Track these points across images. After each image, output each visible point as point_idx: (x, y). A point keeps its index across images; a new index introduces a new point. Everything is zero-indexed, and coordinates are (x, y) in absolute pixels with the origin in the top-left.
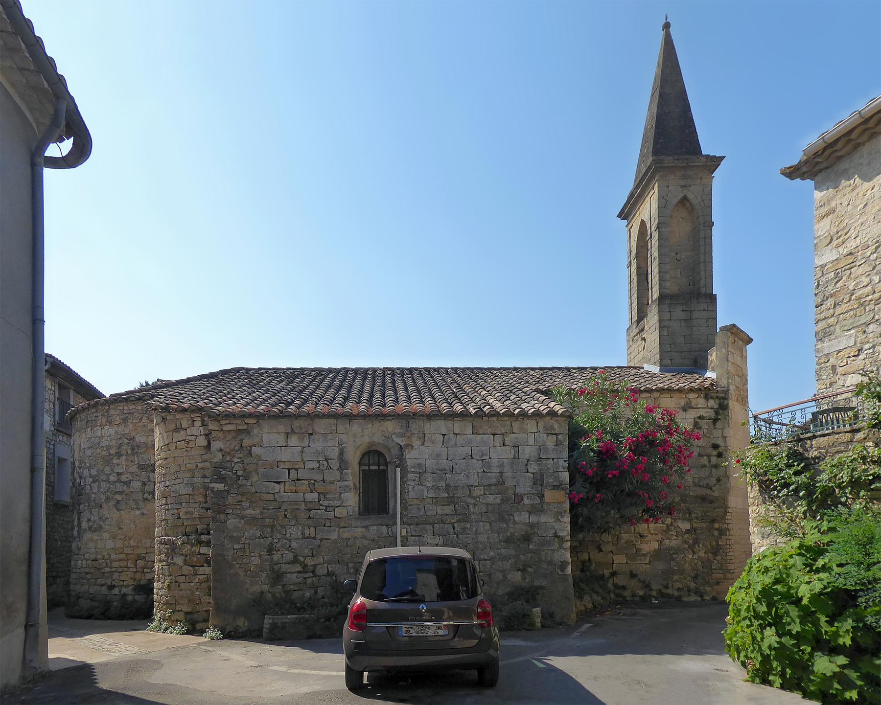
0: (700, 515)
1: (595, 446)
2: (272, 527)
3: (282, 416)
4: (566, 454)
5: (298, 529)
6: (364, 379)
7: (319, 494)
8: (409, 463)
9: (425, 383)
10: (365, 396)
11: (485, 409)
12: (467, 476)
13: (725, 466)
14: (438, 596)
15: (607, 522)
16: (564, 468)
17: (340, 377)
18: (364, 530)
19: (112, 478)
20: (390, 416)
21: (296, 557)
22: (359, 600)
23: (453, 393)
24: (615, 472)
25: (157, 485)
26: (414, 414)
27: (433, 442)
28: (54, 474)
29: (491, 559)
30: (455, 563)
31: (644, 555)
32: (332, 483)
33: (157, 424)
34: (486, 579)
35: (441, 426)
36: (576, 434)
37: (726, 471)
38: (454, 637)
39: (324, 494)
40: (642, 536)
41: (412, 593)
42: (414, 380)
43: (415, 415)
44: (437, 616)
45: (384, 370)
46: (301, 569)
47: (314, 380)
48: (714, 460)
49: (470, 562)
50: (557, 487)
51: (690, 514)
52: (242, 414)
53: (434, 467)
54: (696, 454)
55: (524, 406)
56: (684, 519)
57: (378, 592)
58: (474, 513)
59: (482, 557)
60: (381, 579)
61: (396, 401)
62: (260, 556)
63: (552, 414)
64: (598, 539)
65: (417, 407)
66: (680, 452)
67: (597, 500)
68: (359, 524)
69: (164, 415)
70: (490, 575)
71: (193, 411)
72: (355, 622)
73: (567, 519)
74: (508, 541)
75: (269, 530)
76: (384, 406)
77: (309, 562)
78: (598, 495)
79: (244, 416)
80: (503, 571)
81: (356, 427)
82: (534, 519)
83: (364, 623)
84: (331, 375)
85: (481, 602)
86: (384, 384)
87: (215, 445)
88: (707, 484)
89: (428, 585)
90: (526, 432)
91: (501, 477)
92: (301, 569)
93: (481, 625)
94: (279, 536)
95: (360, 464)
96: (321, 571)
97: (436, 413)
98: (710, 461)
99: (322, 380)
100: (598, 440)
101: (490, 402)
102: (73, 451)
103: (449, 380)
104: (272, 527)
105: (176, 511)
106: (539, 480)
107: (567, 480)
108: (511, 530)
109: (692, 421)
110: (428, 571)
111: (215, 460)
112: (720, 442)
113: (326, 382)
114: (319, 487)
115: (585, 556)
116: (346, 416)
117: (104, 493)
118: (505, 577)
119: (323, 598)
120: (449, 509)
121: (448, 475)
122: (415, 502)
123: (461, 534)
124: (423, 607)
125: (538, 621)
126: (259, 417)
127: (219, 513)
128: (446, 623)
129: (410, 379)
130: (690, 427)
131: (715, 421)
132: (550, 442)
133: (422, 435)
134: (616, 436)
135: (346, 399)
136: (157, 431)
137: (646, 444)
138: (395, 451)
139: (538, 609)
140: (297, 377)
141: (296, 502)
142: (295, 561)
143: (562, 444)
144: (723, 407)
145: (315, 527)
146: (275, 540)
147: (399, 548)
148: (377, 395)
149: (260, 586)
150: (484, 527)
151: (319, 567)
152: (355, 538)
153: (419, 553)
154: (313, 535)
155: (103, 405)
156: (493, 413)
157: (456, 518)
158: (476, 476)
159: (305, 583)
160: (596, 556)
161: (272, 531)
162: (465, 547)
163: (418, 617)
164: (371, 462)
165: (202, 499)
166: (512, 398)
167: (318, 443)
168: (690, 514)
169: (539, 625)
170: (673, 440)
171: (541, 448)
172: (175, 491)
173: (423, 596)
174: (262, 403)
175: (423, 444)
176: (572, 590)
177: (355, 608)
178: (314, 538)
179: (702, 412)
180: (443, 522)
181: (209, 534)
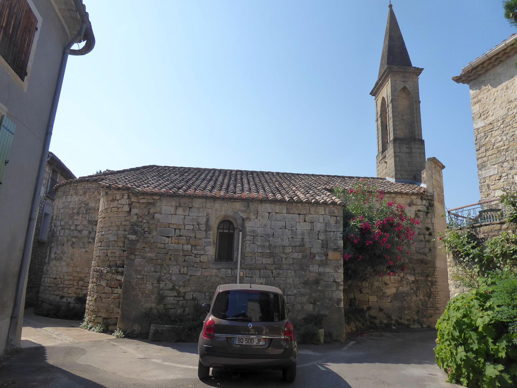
0: (420, 272)
1: (359, 225)
2: (162, 265)
3: (175, 195)
4: (341, 229)
5: (177, 268)
6: (225, 176)
7: (192, 246)
8: (248, 229)
9: (260, 181)
10: (224, 186)
11: (294, 198)
12: (282, 240)
13: (434, 241)
14: (260, 318)
15: (365, 274)
16: (340, 238)
17: (211, 174)
18: (217, 271)
19: (73, 228)
20: (238, 199)
21: (174, 286)
22: (211, 318)
23: (276, 187)
24: (370, 242)
25: (97, 234)
26: (253, 199)
27: (262, 217)
28: (41, 223)
29: (295, 295)
30: (272, 296)
31: (388, 296)
32: (200, 239)
33: (103, 196)
34: (290, 308)
35: (268, 207)
36: (347, 217)
37: (434, 245)
38: (269, 347)
39: (195, 246)
40: (386, 284)
41: (244, 315)
42: (253, 178)
43: (253, 200)
44: (259, 332)
45: (237, 171)
46: (176, 294)
47: (195, 175)
48: (427, 237)
49: (281, 296)
50: (335, 250)
51: (414, 271)
52: (151, 193)
53: (263, 233)
54: (417, 233)
55: (317, 198)
56: (411, 274)
57: (223, 313)
58: (285, 264)
59: (289, 293)
60: (225, 304)
61: (242, 190)
62: (152, 284)
63: (334, 203)
64: (360, 285)
65: (254, 195)
66: (408, 231)
67: (359, 260)
68: (214, 267)
69: (107, 191)
70: (293, 306)
71: (124, 190)
72: (207, 333)
73: (341, 271)
74: (306, 283)
75: (159, 267)
76: (235, 193)
77: (182, 290)
78: (360, 256)
79: (153, 194)
80: (302, 303)
81: (217, 205)
82: (321, 270)
83: (212, 334)
84: (206, 173)
85: (287, 323)
86: (236, 180)
87: (134, 211)
88: (424, 252)
89: (254, 310)
90: (318, 214)
91: (302, 241)
92: (176, 294)
93: (286, 340)
94: (165, 272)
95: (218, 228)
96: (189, 296)
97: (265, 199)
98: (425, 238)
99: (200, 175)
100: (360, 221)
101: (298, 194)
102: (53, 209)
103: (274, 179)
104: (162, 265)
105: (106, 251)
106: (325, 245)
107: (342, 245)
108: (308, 276)
109: (414, 212)
110: (255, 301)
111: (132, 220)
112: (430, 226)
113: (203, 176)
114: (192, 241)
115: (352, 296)
116: (212, 198)
117: (66, 237)
118: (302, 307)
119: (188, 315)
120: (270, 261)
121: (271, 239)
122: (250, 254)
123: (277, 277)
124: (250, 325)
125: (322, 338)
126: (161, 195)
127: (131, 254)
128: (264, 337)
129: (251, 178)
130: (413, 216)
131: (427, 213)
132: (332, 221)
133: (256, 212)
134: (371, 219)
135: (213, 187)
136: (102, 200)
137: (388, 226)
138: (239, 221)
139: (322, 331)
140: (186, 172)
141: (177, 250)
142: (173, 289)
143: (339, 223)
144: (431, 205)
145: (187, 267)
146: (163, 274)
147: (238, 284)
148: (232, 186)
149: (149, 304)
150: (291, 273)
151: (187, 294)
152: (211, 276)
153: (250, 289)
154: (185, 272)
155: (74, 183)
156: (299, 201)
157: (274, 266)
158: (287, 240)
159: (178, 304)
160: (359, 297)
161: (161, 268)
162: (279, 286)
163: (246, 331)
164: (225, 227)
165: (122, 245)
166: (310, 192)
167: (194, 214)
168: (414, 271)
169: (322, 341)
170: (404, 223)
171: (327, 224)
172: (107, 239)
173: (251, 317)
174: (164, 187)
175: (257, 218)
176: (343, 318)
177: (208, 323)
178: (186, 274)
179: (420, 208)
180: (266, 269)
181: (123, 267)
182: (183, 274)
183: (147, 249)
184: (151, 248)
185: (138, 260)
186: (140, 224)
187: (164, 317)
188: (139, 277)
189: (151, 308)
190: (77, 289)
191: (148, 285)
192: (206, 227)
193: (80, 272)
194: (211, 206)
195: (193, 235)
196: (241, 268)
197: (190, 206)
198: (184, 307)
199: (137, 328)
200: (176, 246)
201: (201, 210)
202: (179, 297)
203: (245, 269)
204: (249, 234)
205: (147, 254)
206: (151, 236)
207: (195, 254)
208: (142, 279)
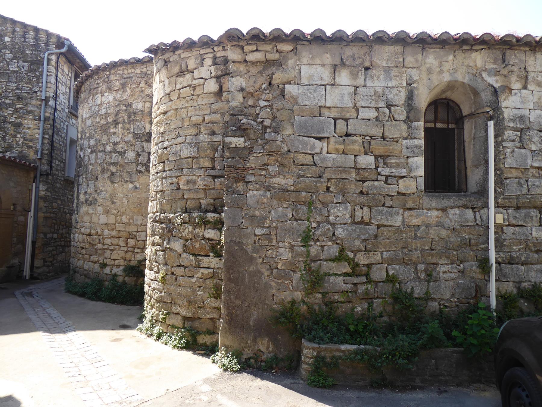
5: (346, 208)
7: (376, 157)
8: (507, 114)
18: (439, 213)
32: (396, 141)
39: (385, 157)
46: (349, 270)
62: (292, 247)
77: (362, 259)
92: (349, 270)
94: (319, 218)
96: (378, 274)
104: (310, 204)
114: (378, 147)
122: (515, 173)
133: (523, 74)
138: (486, 96)
141: (343, 169)
142: (341, 257)
145: (370, 207)
146: (314, 225)
149: (290, 292)
151: (375, 268)
152: (428, 226)
154: (366, 219)
159: (355, 292)
175: (525, 87)
178: (367, 224)
182: (361, 222)
183: (273, 169)
184: (282, 166)
185: (254, 195)
186: (252, 111)
187: (326, 323)
188: (259, 231)
189: (293, 302)
190: (126, 252)
191: (281, 250)
192: (408, 112)
193: (129, 224)
194: (417, 61)
195: (377, 132)
196: (497, 205)
197: (367, 64)
198: (368, 298)
199: (265, 347)
200: (339, 158)
201: (394, 72)
202: (357, 276)
203: (505, 207)
204: (511, 124)
205: (274, 180)
206: (279, 138)
207: (387, 177)
208: (268, 237)
